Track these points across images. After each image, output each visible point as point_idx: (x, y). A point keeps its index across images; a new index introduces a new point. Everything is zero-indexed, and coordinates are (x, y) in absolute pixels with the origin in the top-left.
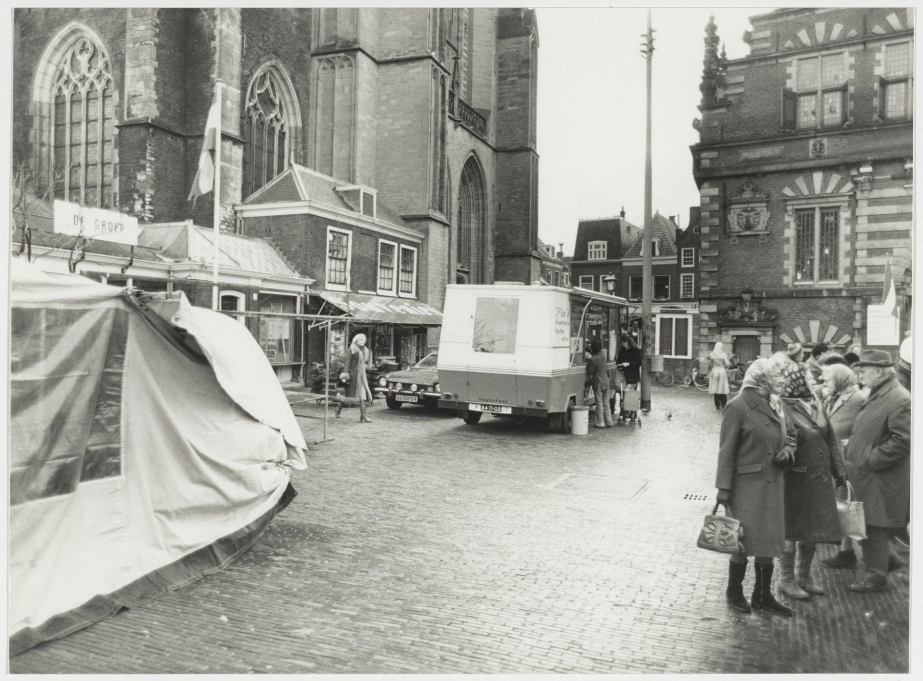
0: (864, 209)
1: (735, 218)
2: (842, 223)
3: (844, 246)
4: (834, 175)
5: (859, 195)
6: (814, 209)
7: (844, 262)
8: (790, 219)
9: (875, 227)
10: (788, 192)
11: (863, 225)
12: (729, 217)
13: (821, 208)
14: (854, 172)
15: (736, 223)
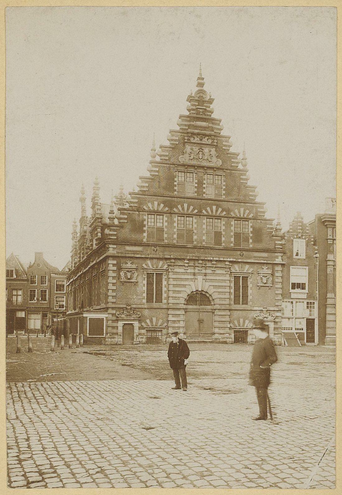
0: (171, 275)
1: (124, 274)
2: (164, 280)
3: (164, 289)
4: (161, 261)
5: (170, 270)
6: (153, 273)
7: (164, 295)
8: (146, 276)
9: (175, 283)
10: (144, 265)
11: (171, 282)
12: (121, 273)
13: (156, 273)
14: (168, 261)
15: (124, 276)
